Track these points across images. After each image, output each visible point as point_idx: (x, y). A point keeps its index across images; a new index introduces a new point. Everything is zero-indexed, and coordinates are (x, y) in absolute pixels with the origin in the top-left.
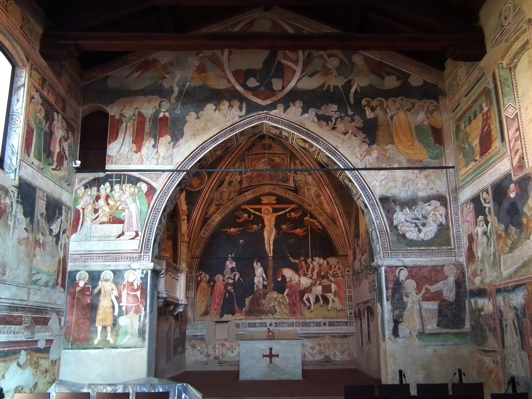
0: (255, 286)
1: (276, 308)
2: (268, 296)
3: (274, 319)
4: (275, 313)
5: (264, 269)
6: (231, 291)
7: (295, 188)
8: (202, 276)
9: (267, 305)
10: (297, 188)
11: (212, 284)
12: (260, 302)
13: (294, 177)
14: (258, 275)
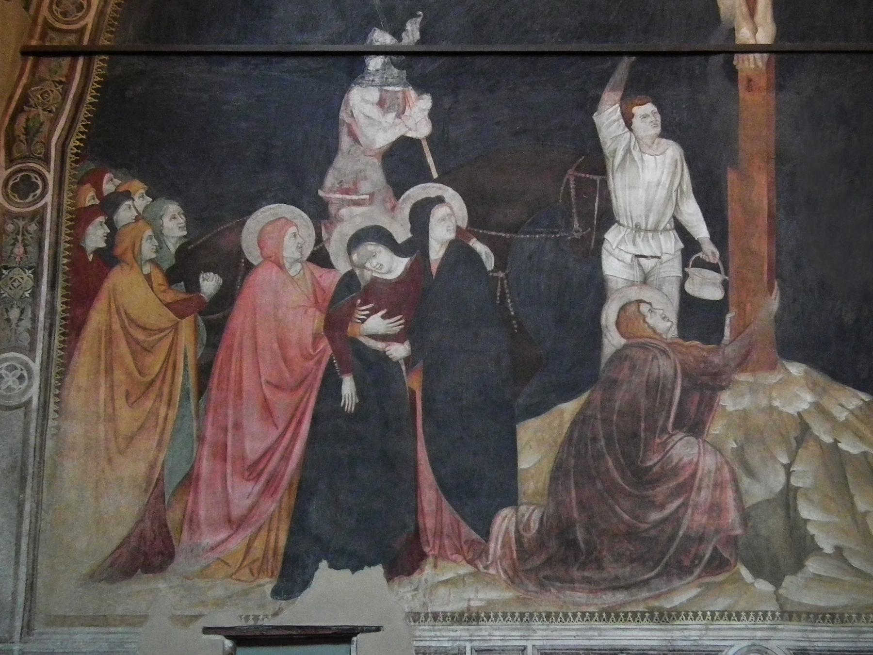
0: (610, 314)
1: (806, 511)
2: (727, 401)
3: (788, 614)
4: (799, 565)
5: (691, 159)
6: (382, 357)
8: (125, 214)
9: (718, 485)
11: (210, 284)
12: (653, 459)
14: (638, 211)
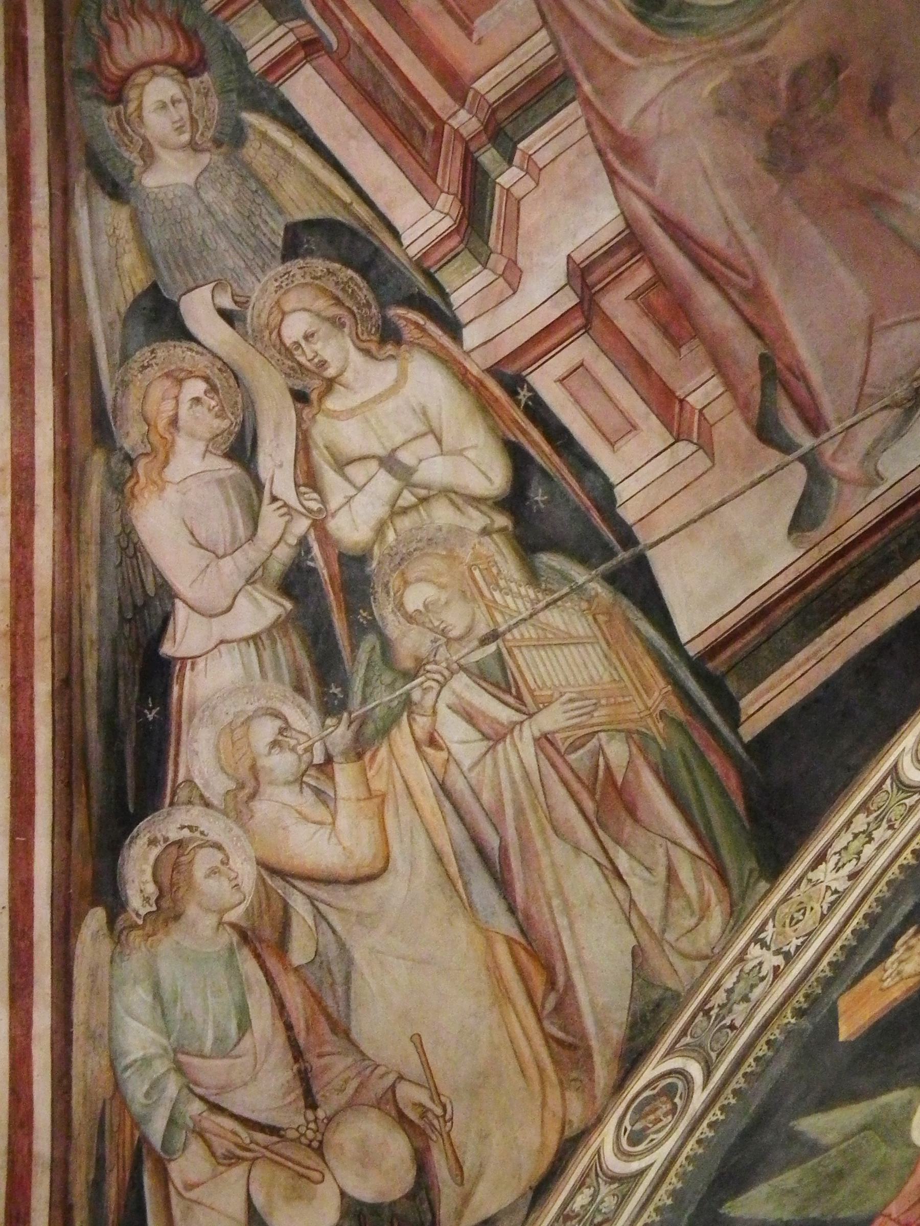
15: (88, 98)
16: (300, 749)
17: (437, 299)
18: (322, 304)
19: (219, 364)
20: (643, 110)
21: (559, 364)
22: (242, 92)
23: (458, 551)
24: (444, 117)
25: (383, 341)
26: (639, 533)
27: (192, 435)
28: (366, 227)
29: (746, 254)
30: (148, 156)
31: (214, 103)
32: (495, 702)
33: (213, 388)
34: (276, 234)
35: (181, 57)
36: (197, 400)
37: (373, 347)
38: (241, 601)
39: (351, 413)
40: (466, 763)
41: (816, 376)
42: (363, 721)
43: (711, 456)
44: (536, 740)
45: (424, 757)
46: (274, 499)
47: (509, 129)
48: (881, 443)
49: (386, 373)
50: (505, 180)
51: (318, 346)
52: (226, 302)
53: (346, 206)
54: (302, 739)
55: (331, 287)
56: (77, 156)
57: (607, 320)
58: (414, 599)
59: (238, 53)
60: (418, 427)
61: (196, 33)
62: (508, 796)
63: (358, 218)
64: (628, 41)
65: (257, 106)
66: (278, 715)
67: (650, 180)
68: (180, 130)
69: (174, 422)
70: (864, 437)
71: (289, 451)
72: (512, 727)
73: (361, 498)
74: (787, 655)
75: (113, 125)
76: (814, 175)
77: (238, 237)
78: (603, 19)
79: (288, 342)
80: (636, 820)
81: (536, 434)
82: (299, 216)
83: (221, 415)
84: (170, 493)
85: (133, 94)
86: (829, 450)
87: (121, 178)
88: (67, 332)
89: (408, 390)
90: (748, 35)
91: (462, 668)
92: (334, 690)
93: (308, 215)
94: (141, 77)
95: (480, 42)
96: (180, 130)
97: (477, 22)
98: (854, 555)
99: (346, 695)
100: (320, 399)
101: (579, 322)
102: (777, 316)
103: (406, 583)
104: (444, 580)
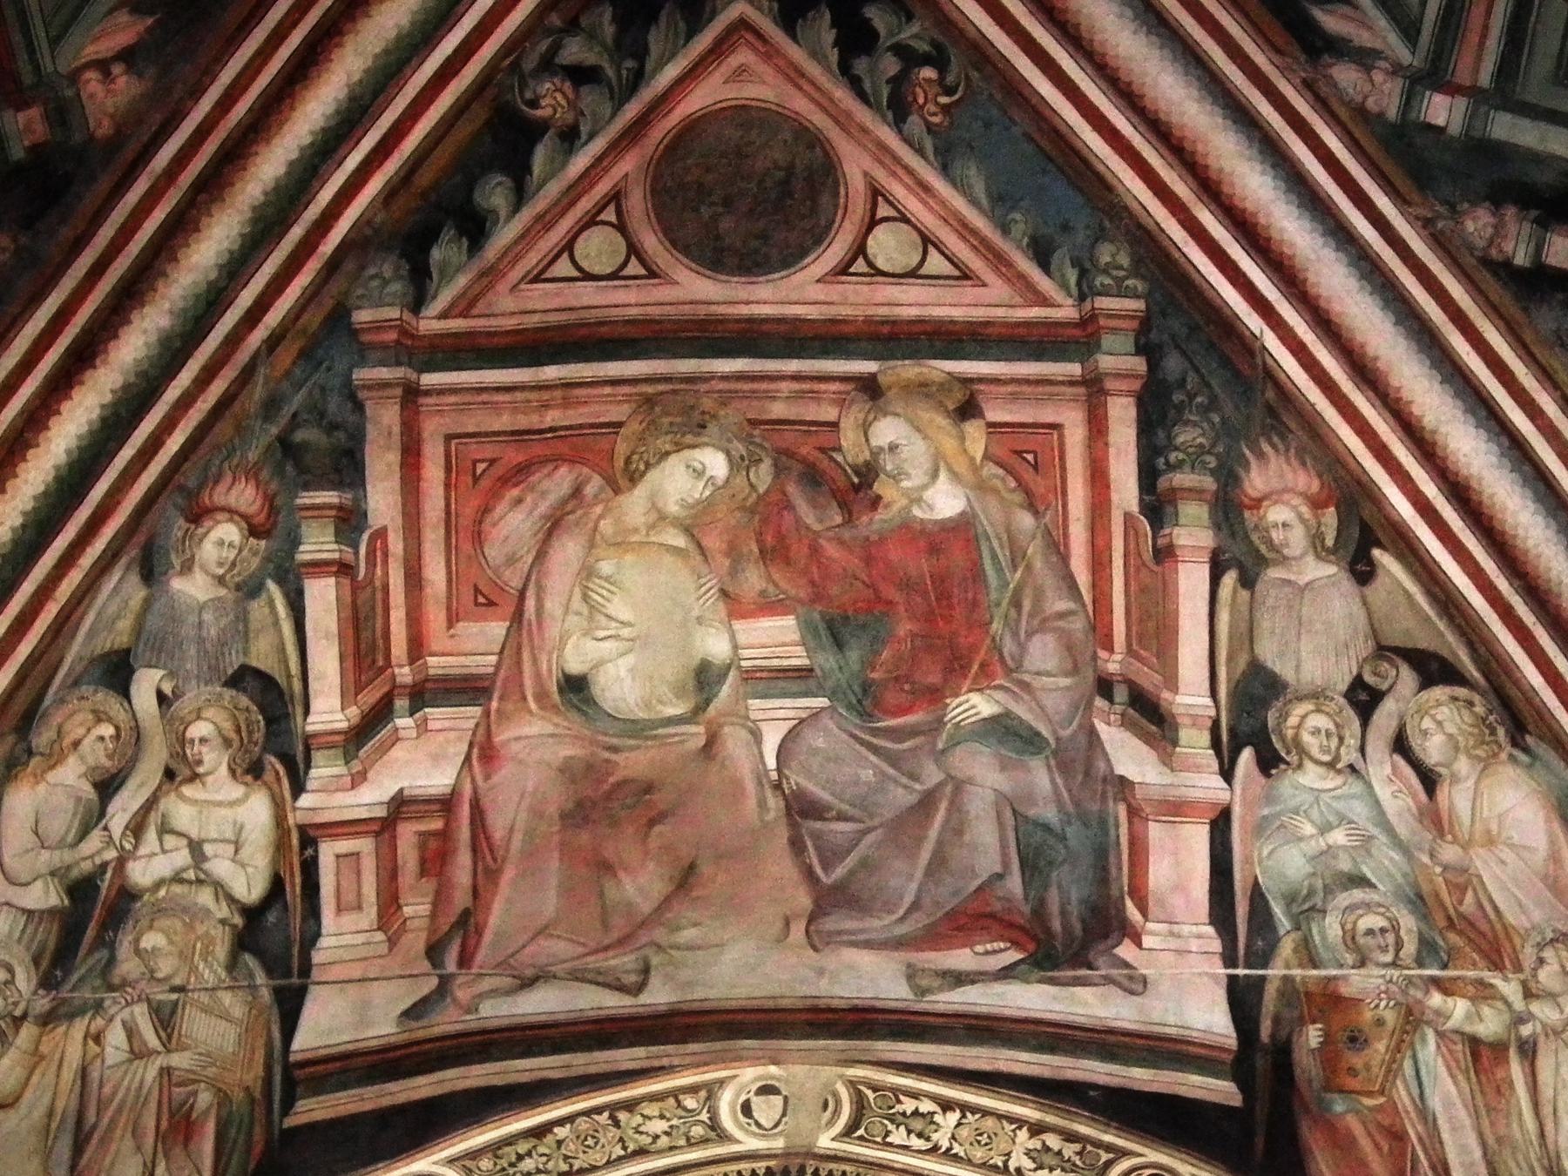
7: (1241, 1066)
10: (1282, 1052)
13: (1221, 823)
15: (175, 505)
16: (10, 1000)
17: (302, 766)
18: (227, 726)
19: (133, 724)
20: (517, 739)
21: (344, 846)
22: (279, 567)
23: (198, 925)
24: (394, 661)
25: (247, 772)
26: (316, 974)
27: (82, 758)
28: (292, 697)
29: (507, 851)
30: (187, 568)
31: (255, 563)
32: (152, 1031)
33: (117, 736)
34: (233, 662)
35: (256, 521)
36: (102, 738)
37: (239, 771)
38: (39, 884)
39: (195, 802)
40: (109, 1062)
41: (488, 937)
42: (64, 1001)
43: (390, 950)
44: (162, 1069)
45: (85, 1044)
46: (106, 828)
47: (427, 696)
48: (494, 993)
49: (237, 791)
50: (400, 722)
51: (204, 749)
52: (167, 688)
53: (289, 676)
54: (16, 995)
55: (242, 718)
56: (140, 538)
57: (394, 838)
58: (151, 940)
59: (295, 542)
60: (229, 835)
61: (278, 513)
62: (120, 1095)
63: (290, 687)
64: (542, 696)
65: (281, 582)
66: (10, 970)
67: (487, 777)
68: (220, 564)
69: (76, 744)
70: (486, 984)
71: (136, 804)
72: (154, 1053)
73: (161, 858)
74: (344, 1086)
75: (180, 534)
76: (584, 838)
77: (206, 652)
78: (538, 675)
79: (189, 734)
80: (186, 1146)
81: (298, 880)
82: (254, 663)
83: (110, 757)
84: (42, 788)
85: (207, 523)
86: (460, 980)
87: (157, 570)
88: (49, 645)
89: (241, 813)
90: (615, 741)
91: (149, 1001)
92: (58, 973)
93: (262, 667)
94: (220, 516)
95: (452, 636)
96: (220, 564)
97: (461, 624)
98: (428, 1046)
99: (63, 980)
100: (181, 783)
101: (376, 828)
102: (494, 894)
103: (151, 927)
104: (177, 938)
